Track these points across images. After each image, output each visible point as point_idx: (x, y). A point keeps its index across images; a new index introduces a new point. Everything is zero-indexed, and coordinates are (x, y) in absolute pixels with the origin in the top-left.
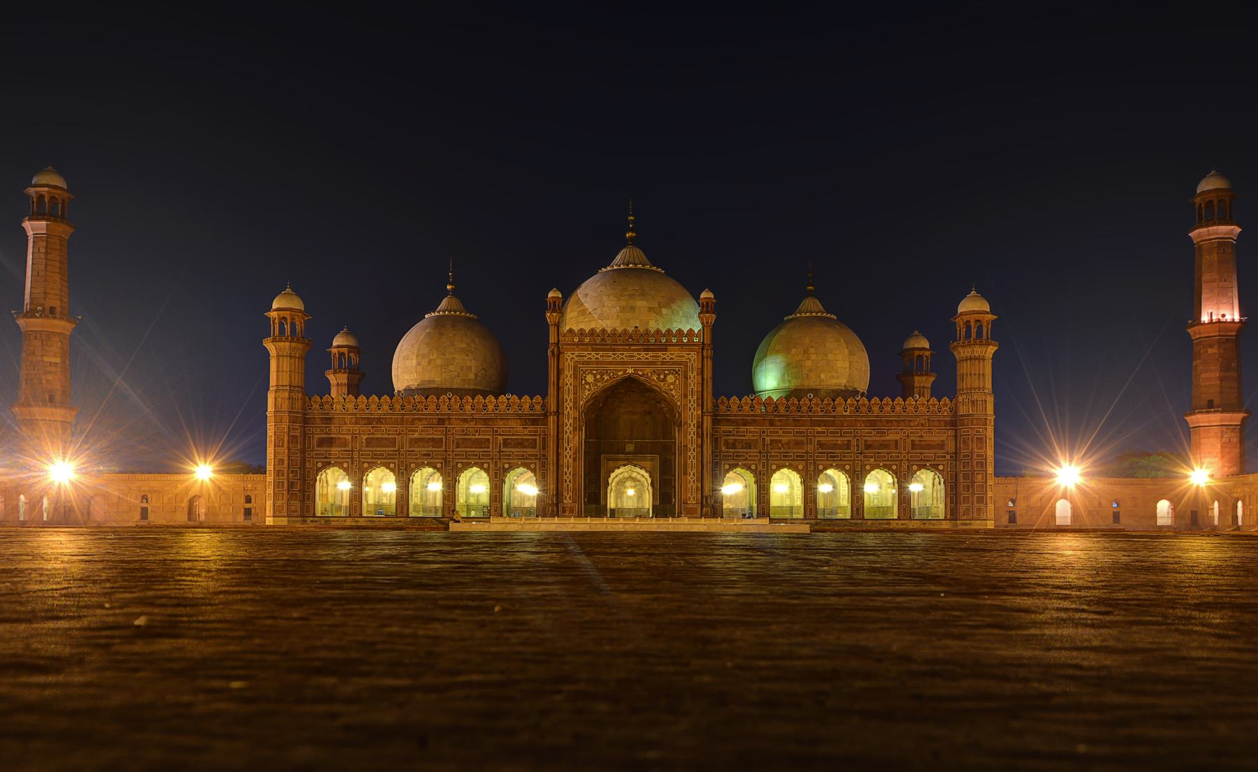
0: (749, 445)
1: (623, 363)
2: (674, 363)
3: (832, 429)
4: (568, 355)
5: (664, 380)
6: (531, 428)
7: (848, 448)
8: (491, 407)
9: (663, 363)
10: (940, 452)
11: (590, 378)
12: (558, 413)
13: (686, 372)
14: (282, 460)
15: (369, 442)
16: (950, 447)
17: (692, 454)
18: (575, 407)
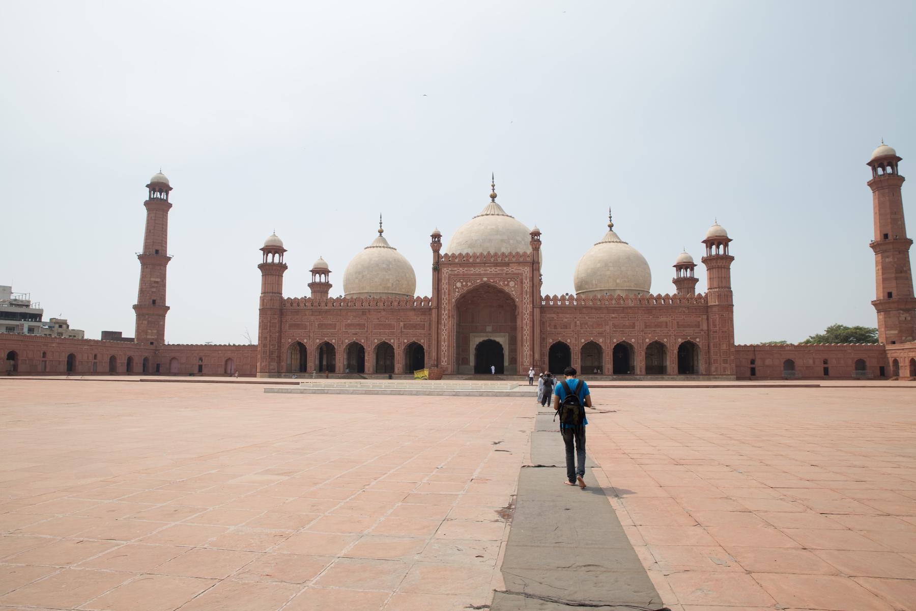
0: (565, 326)
1: (480, 274)
2: (514, 274)
3: (622, 315)
5: (508, 285)
6: (423, 317)
7: (633, 326)
8: (396, 304)
10: (697, 330)
11: (459, 285)
12: (438, 307)
13: (522, 279)
14: (266, 338)
15: (321, 326)
16: (705, 328)
17: (527, 332)
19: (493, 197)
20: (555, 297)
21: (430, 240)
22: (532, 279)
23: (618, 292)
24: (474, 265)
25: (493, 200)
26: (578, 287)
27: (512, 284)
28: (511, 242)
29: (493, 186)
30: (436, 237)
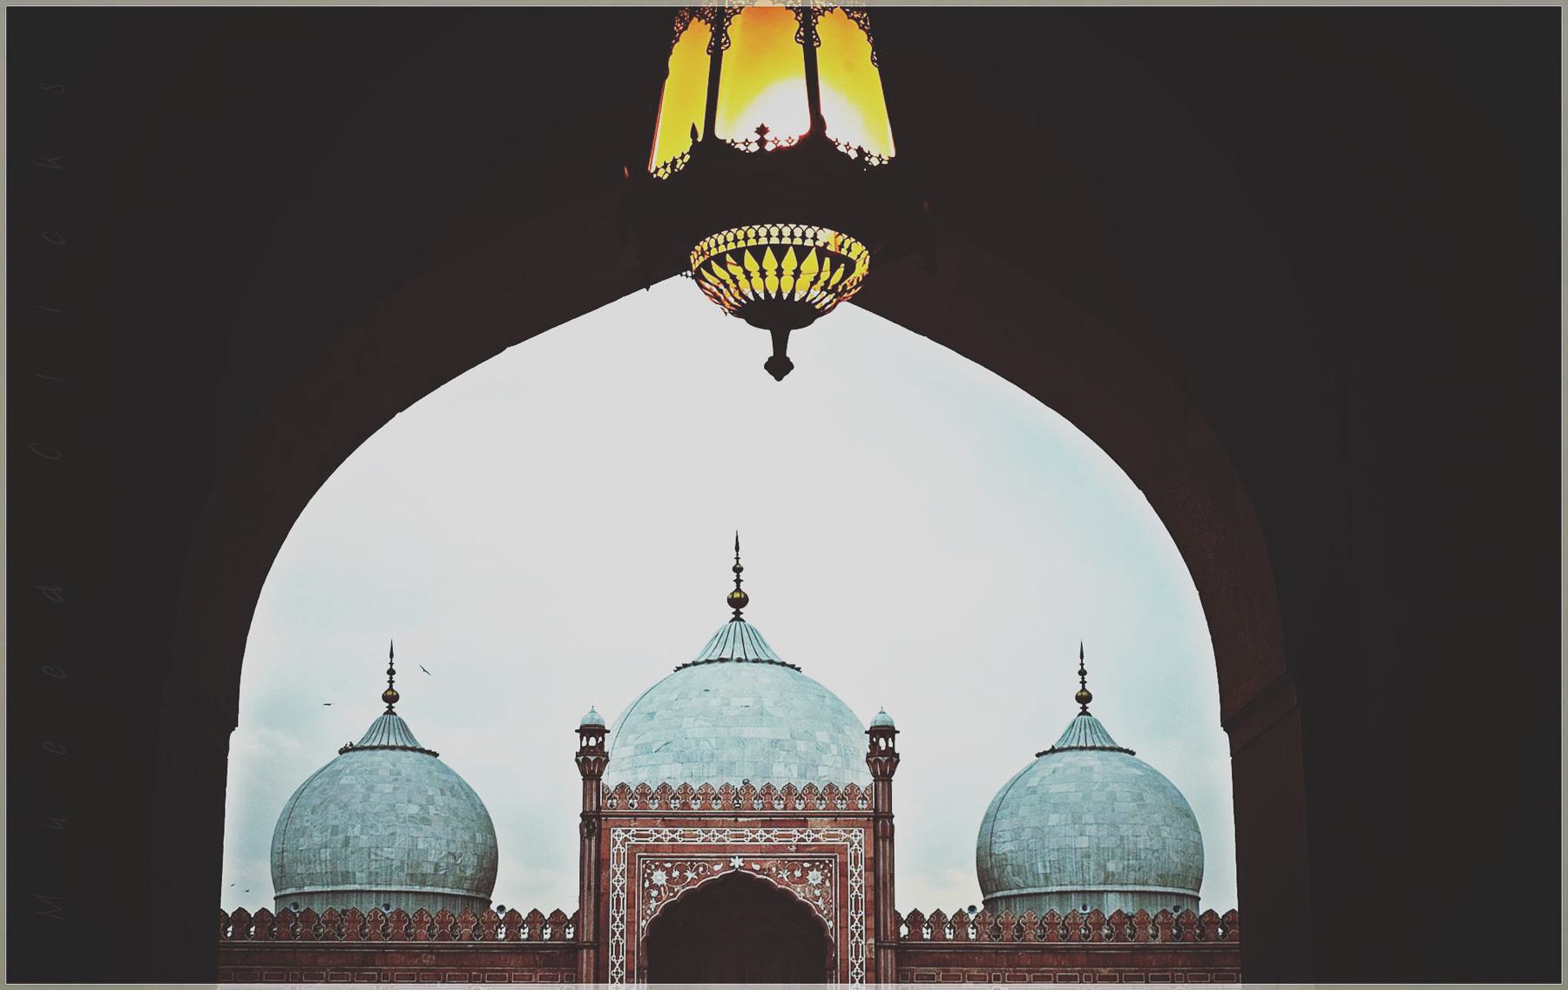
1: (723, 848)
2: (821, 848)
4: (618, 834)
8: (468, 931)
9: (799, 848)
11: (659, 877)
13: (844, 865)
18: (630, 931)
19: (738, 602)
20: (938, 913)
21: (575, 743)
22: (872, 865)
23: (1111, 905)
24: (703, 820)
25: (737, 617)
26: (987, 878)
27: (814, 877)
28: (802, 746)
29: (738, 570)
30: (592, 730)
